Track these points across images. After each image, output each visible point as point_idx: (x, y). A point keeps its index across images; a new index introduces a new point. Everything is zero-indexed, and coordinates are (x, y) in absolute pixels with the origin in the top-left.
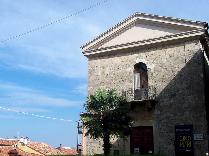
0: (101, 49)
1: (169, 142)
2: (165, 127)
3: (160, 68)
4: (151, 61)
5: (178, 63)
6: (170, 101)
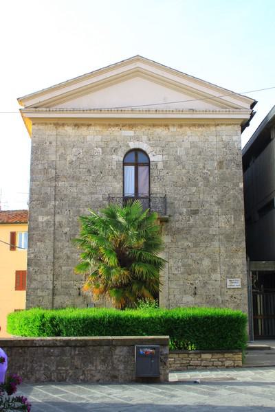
0: (62, 111)
1: (185, 291)
2: (180, 264)
3: (173, 163)
4: (158, 149)
5: (203, 158)
6: (189, 221)
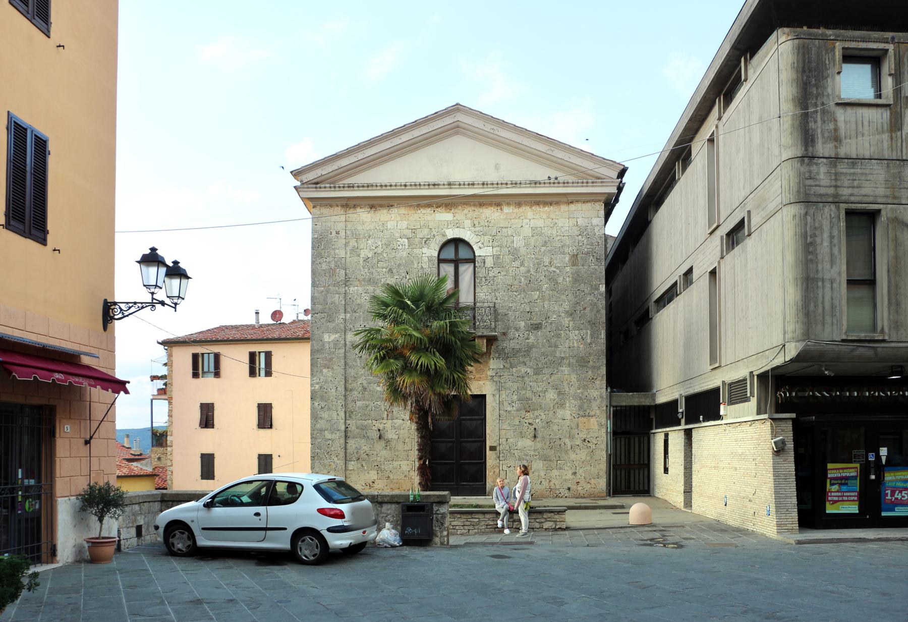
0: (351, 187)
2: (515, 397)
3: (508, 258)
6: (527, 339)
